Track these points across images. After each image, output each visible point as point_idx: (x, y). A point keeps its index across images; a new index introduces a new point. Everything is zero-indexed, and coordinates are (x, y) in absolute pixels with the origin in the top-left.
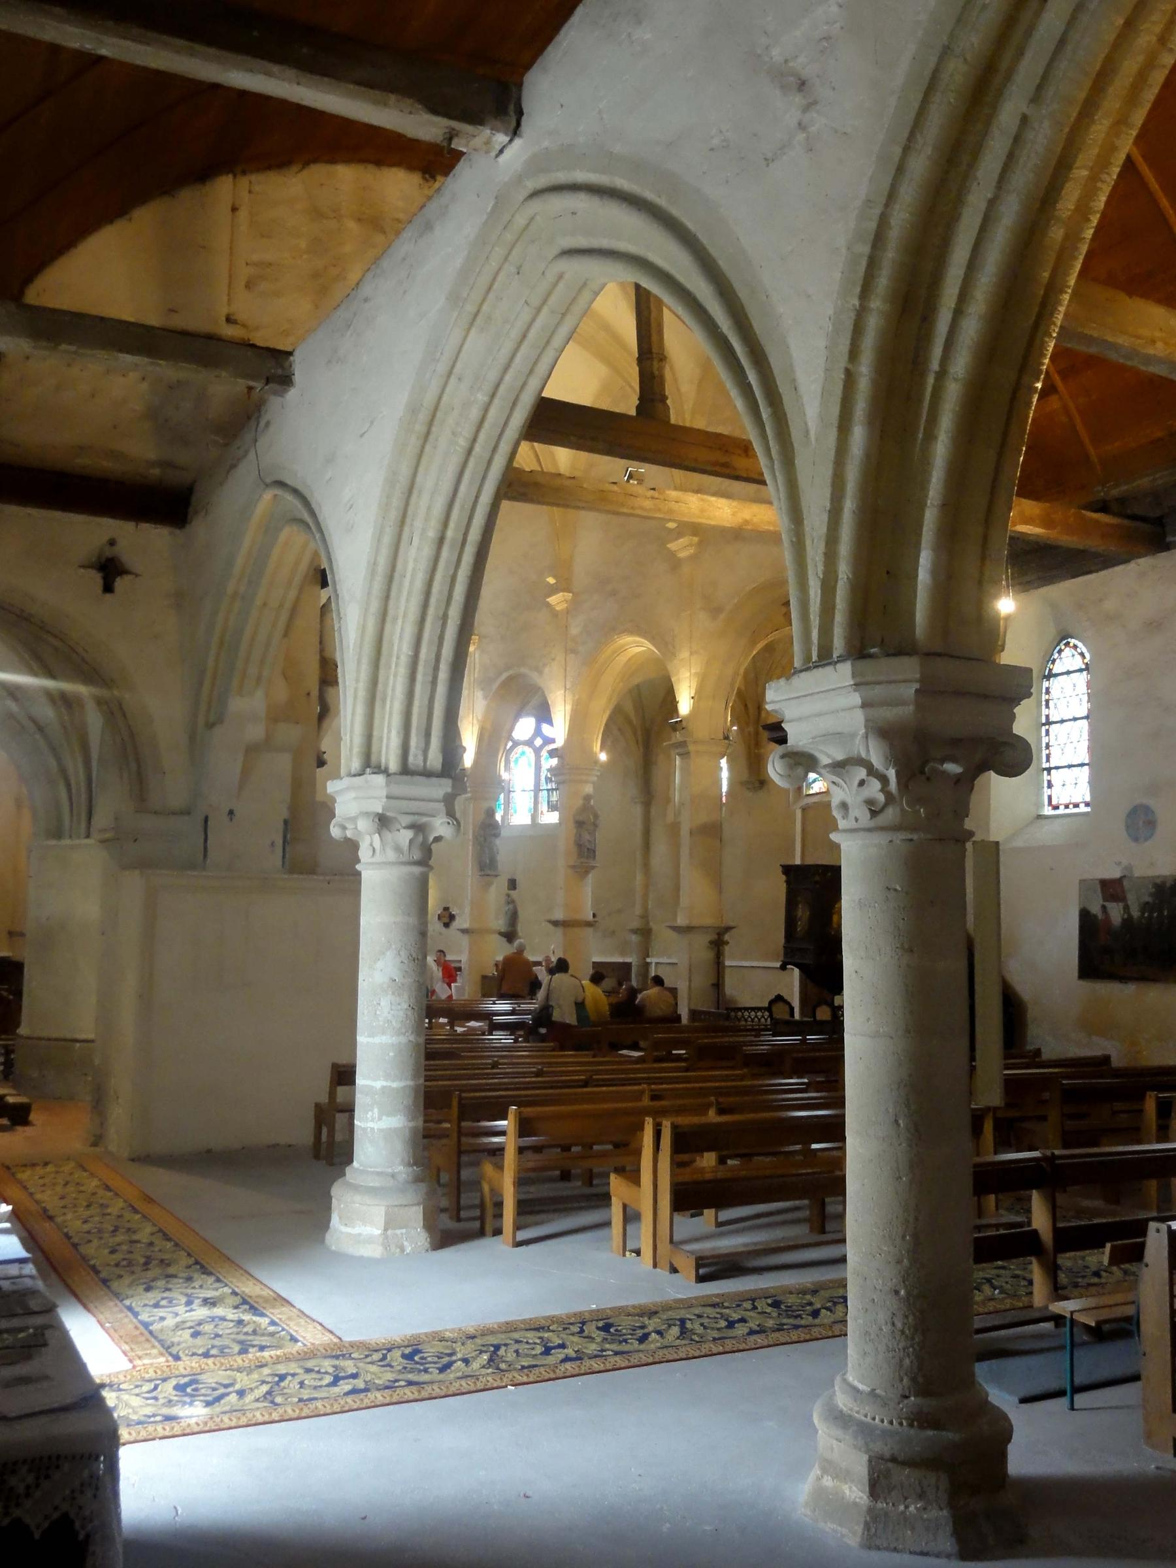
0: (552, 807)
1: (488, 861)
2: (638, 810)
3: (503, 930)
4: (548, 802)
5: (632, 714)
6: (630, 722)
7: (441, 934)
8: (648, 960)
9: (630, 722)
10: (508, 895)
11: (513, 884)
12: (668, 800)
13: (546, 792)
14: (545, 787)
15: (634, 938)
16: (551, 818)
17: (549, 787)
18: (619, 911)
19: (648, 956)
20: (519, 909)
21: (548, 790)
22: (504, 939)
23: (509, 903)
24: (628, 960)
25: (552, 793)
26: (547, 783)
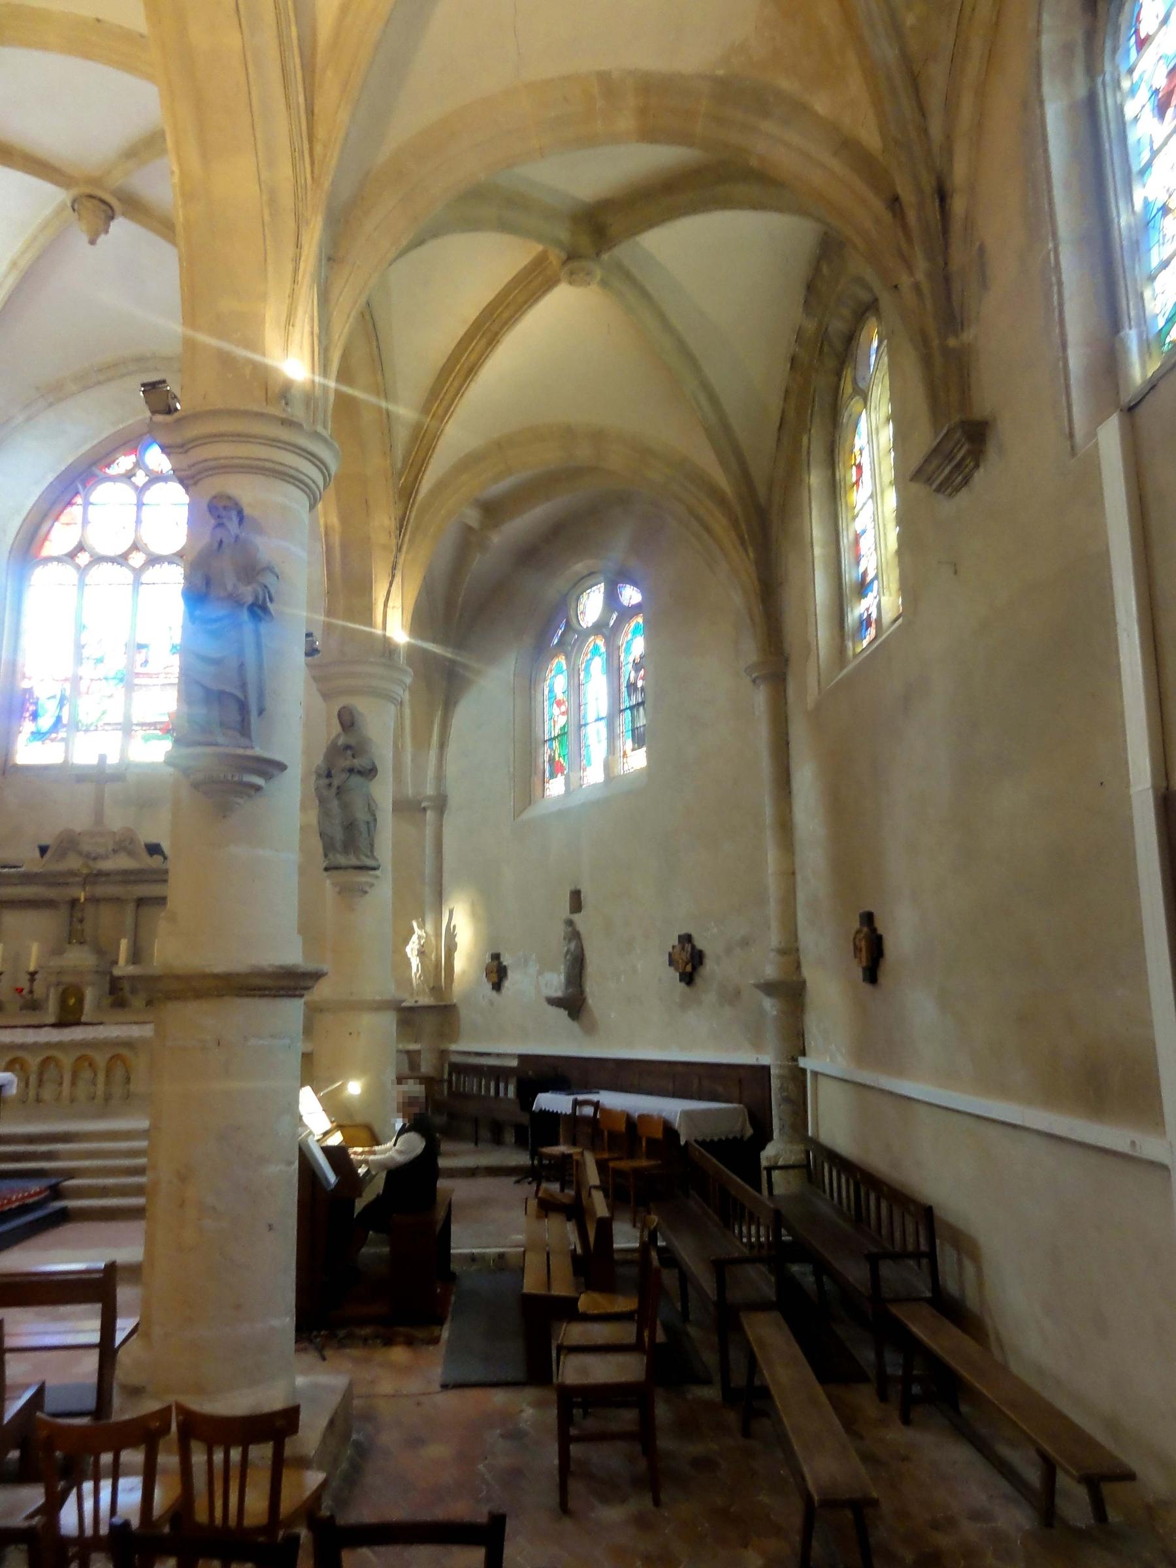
0: (639, 739)
1: (339, 835)
2: (760, 698)
3: (559, 994)
4: (633, 730)
5: (722, 481)
6: (721, 500)
7: (491, 1003)
8: (803, 1062)
9: (721, 500)
10: (570, 923)
11: (577, 901)
12: (808, 648)
13: (628, 712)
14: (627, 704)
15: (770, 1005)
16: (637, 760)
17: (634, 702)
18: (745, 943)
19: (804, 1054)
20: (589, 954)
21: (631, 708)
22: (563, 1013)
23: (570, 941)
24: (765, 1060)
25: (638, 711)
26: (629, 695)
